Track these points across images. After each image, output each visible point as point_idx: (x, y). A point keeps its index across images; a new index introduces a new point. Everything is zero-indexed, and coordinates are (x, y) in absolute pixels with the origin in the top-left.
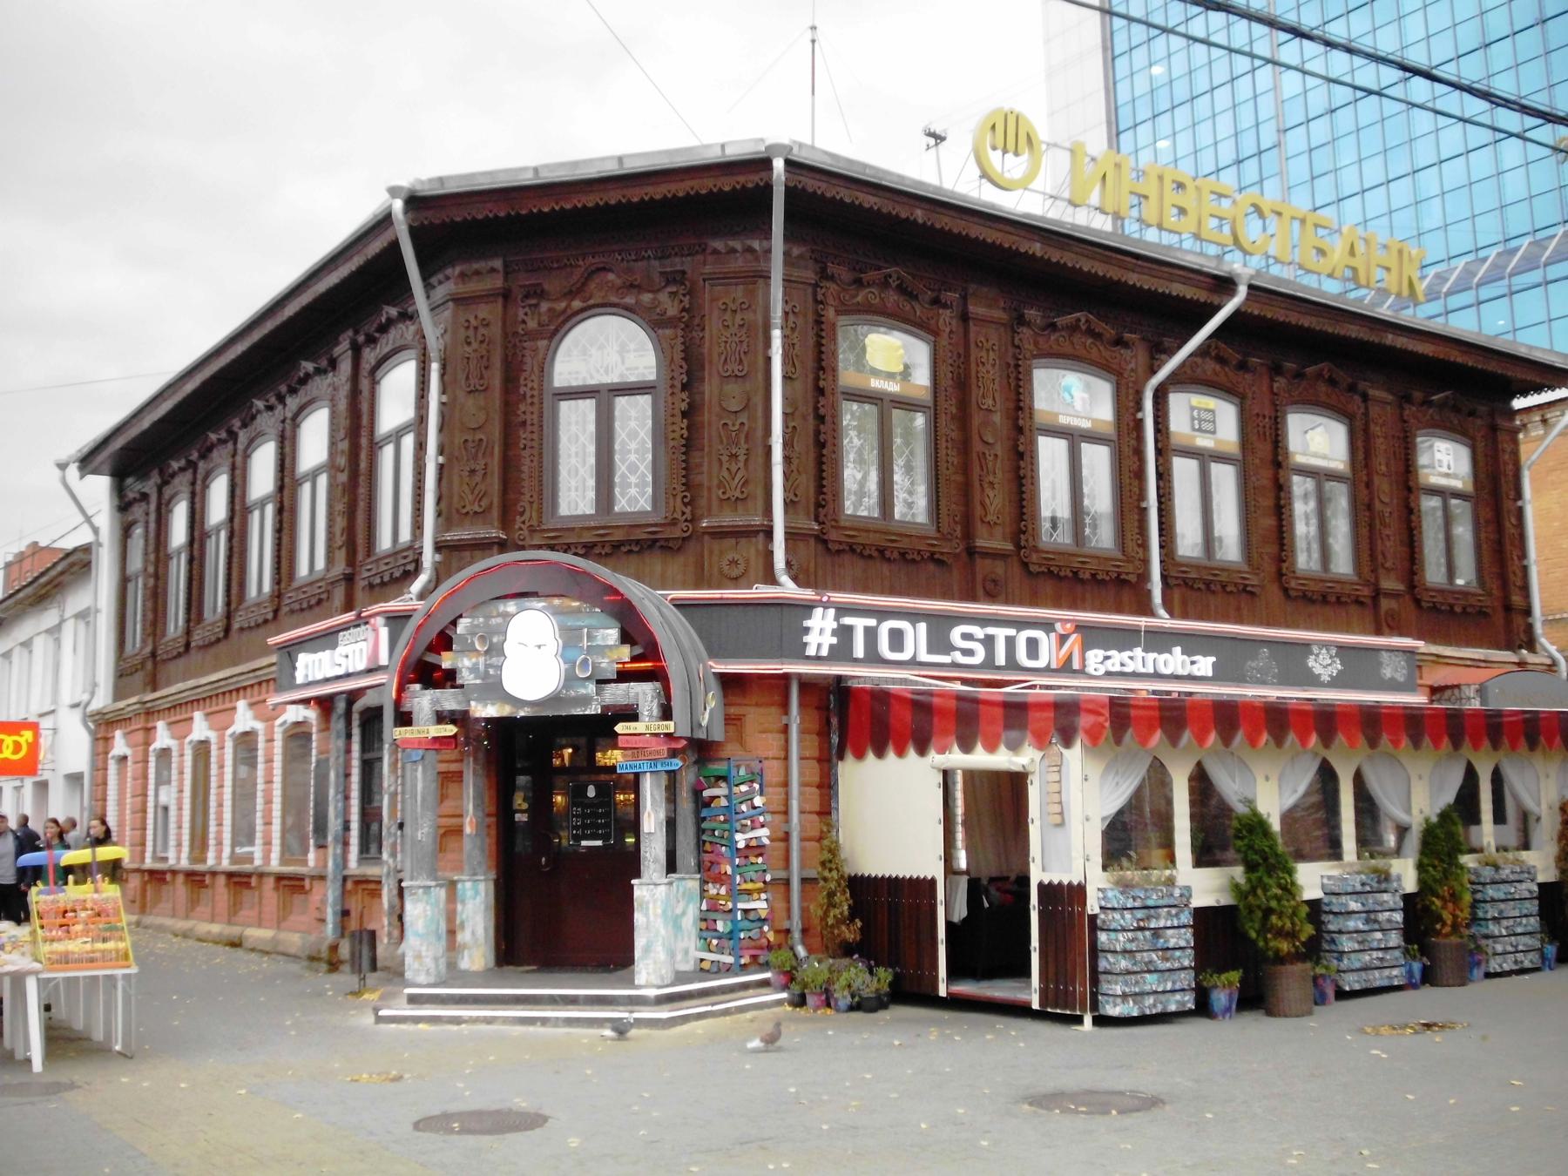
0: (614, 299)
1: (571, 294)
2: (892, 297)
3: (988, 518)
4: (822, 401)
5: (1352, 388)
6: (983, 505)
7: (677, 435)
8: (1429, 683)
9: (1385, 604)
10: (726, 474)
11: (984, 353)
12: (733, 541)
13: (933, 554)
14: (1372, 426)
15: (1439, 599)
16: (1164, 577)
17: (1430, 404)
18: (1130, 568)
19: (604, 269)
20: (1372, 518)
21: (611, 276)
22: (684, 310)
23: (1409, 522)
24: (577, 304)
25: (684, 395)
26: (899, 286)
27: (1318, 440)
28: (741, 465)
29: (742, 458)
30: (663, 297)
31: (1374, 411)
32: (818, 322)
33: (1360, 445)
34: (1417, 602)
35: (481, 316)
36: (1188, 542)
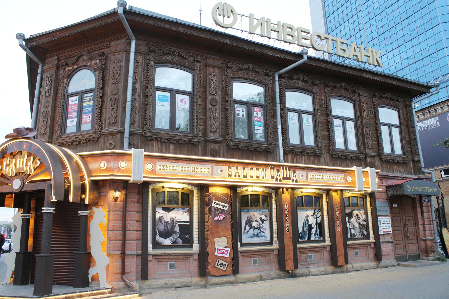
0: (85, 64)
1: (74, 64)
2: (176, 59)
3: (213, 130)
4: (147, 90)
5: (354, 92)
6: (211, 126)
7: (98, 104)
8: (385, 185)
9: (369, 160)
10: (110, 115)
11: (212, 77)
12: (111, 137)
13: (190, 141)
14: (362, 104)
15: (389, 158)
16: (284, 150)
17: (382, 97)
18: (270, 147)
19: (81, 56)
20: (363, 132)
21: (85, 57)
22: (103, 64)
23: (377, 134)
24: (75, 67)
25: (101, 91)
26: (179, 55)
27: (342, 108)
28: (115, 111)
29: (115, 109)
30: (98, 61)
31: (363, 99)
32: (147, 65)
33: (358, 110)
34: (381, 159)
35: (51, 73)
36: (294, 139)
